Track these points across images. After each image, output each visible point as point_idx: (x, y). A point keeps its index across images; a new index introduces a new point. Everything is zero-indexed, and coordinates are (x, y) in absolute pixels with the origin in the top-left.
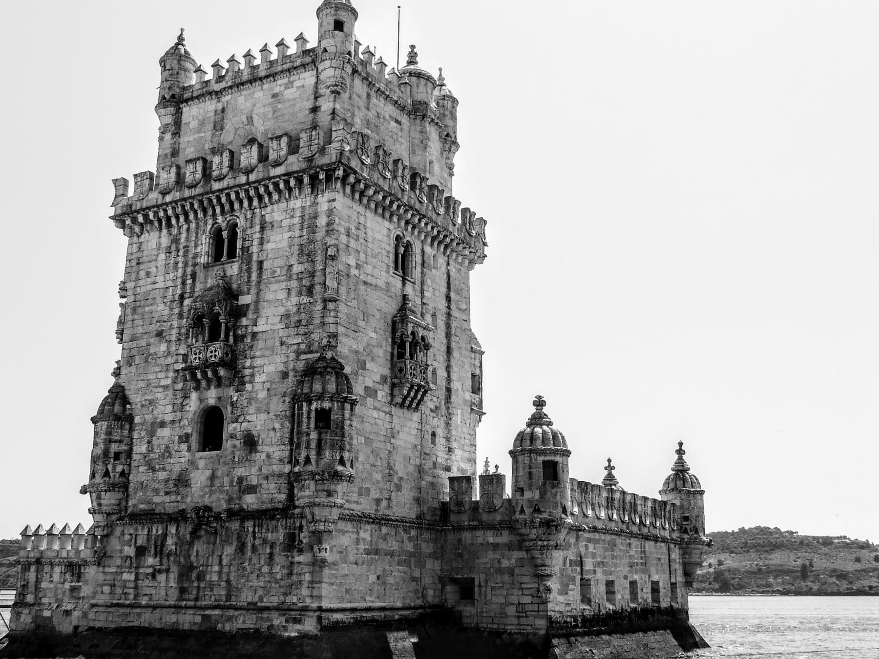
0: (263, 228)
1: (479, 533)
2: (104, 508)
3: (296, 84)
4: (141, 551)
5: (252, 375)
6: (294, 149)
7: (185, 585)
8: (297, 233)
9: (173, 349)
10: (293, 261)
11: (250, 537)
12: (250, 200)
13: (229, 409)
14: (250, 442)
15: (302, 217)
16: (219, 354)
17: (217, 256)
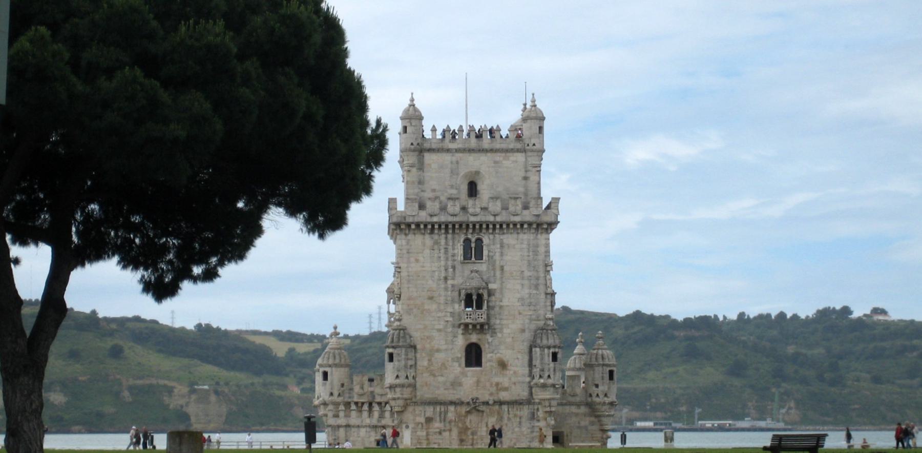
0: (502, 246)
1: (568, 407)
2: (405, 396)
3: (512, 158)
4: (429, 420)
5: (501, 329)
6: (526, 207)
7: (464, 438)
8: (526, 254)
9: (442, 307)
10: (524, 268)
11: (506, 413)
12: (494, 228)
13: (487, 346)
14: (503, 365)
15: (529, 245)
16: (485, 316)
17: (467, 256)
